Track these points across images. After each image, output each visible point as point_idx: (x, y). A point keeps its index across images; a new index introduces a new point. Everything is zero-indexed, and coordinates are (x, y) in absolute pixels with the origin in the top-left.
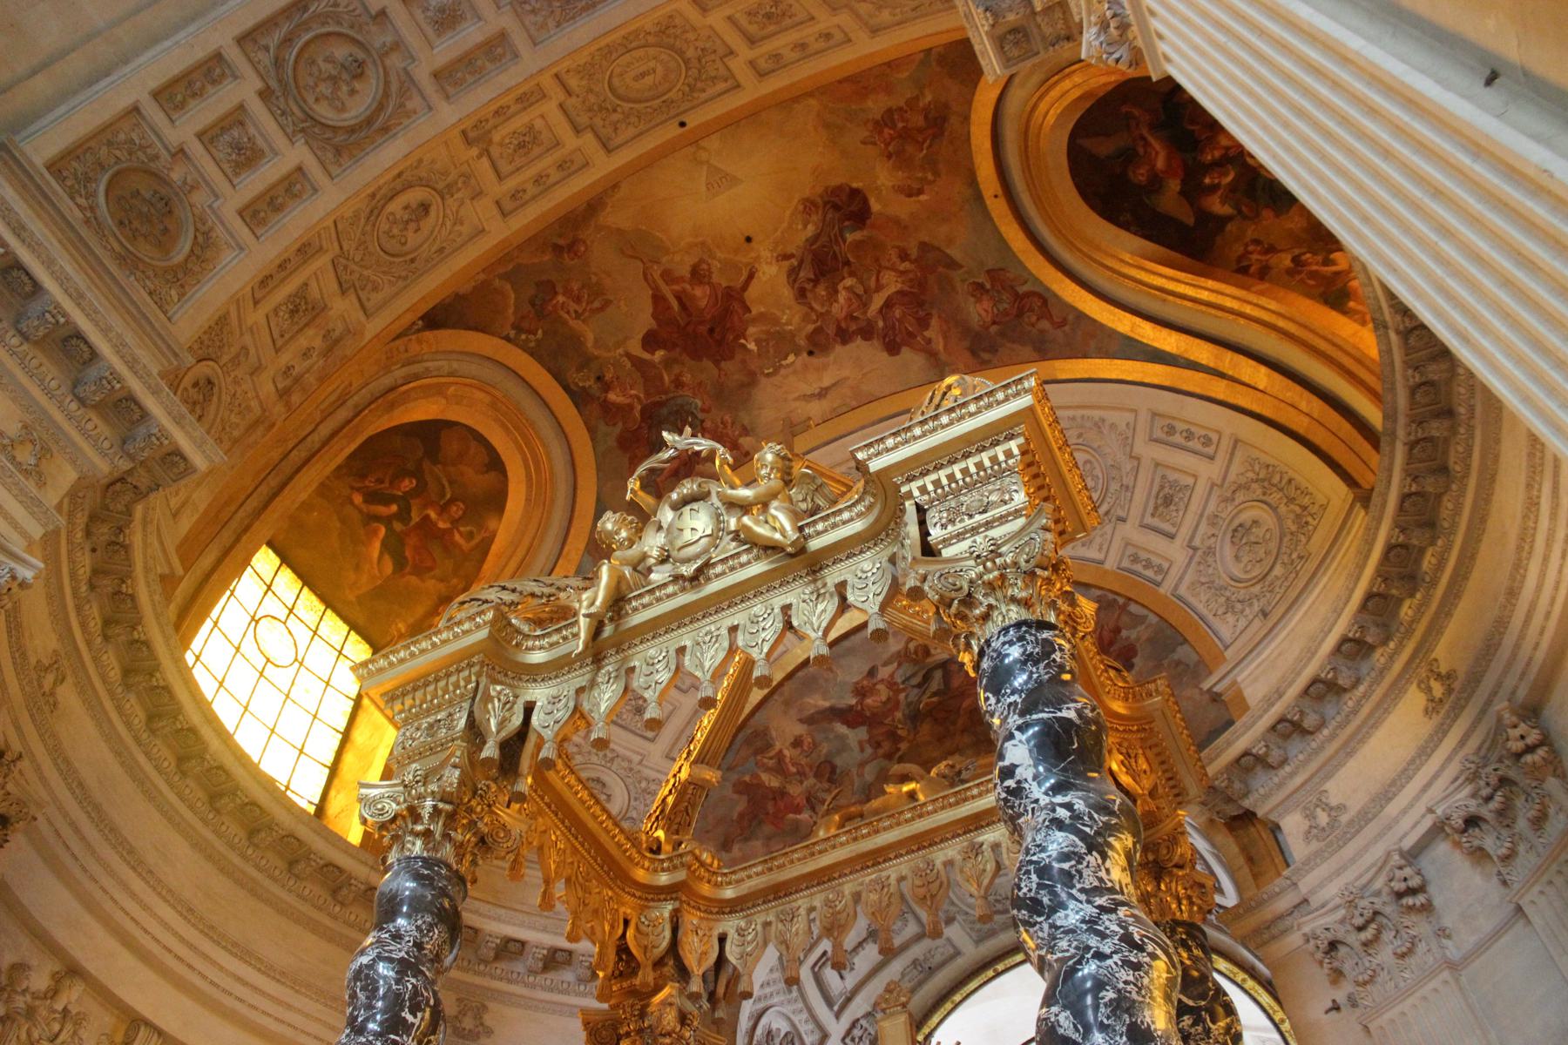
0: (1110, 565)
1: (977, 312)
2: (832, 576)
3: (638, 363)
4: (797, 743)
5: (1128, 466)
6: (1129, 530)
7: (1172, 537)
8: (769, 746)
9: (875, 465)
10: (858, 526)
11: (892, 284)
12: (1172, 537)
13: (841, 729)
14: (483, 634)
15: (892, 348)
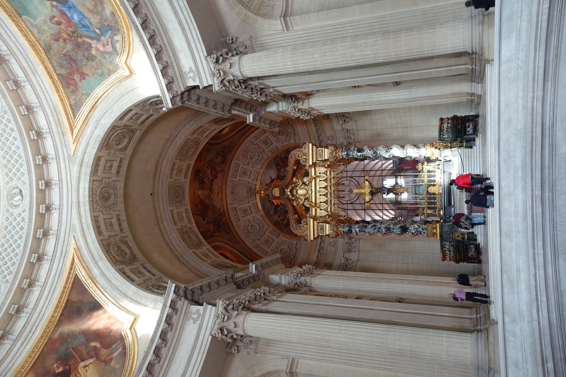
0: (270, 155)
1: (219, 160)
2: (318, 174)
3: (207, 223)
4: (279, 217)
5: (256, 146)
6: (266, 150)
7: (272, 144)
8: (278, 221)
9: (311, 163)
10: (313, 169)
11: (209, 172)
12: (272, 144)
13: (279, 208)
14: (312, 220)
15: (216, 177)
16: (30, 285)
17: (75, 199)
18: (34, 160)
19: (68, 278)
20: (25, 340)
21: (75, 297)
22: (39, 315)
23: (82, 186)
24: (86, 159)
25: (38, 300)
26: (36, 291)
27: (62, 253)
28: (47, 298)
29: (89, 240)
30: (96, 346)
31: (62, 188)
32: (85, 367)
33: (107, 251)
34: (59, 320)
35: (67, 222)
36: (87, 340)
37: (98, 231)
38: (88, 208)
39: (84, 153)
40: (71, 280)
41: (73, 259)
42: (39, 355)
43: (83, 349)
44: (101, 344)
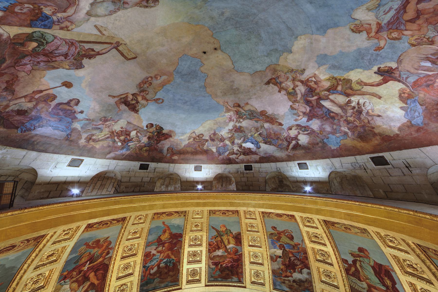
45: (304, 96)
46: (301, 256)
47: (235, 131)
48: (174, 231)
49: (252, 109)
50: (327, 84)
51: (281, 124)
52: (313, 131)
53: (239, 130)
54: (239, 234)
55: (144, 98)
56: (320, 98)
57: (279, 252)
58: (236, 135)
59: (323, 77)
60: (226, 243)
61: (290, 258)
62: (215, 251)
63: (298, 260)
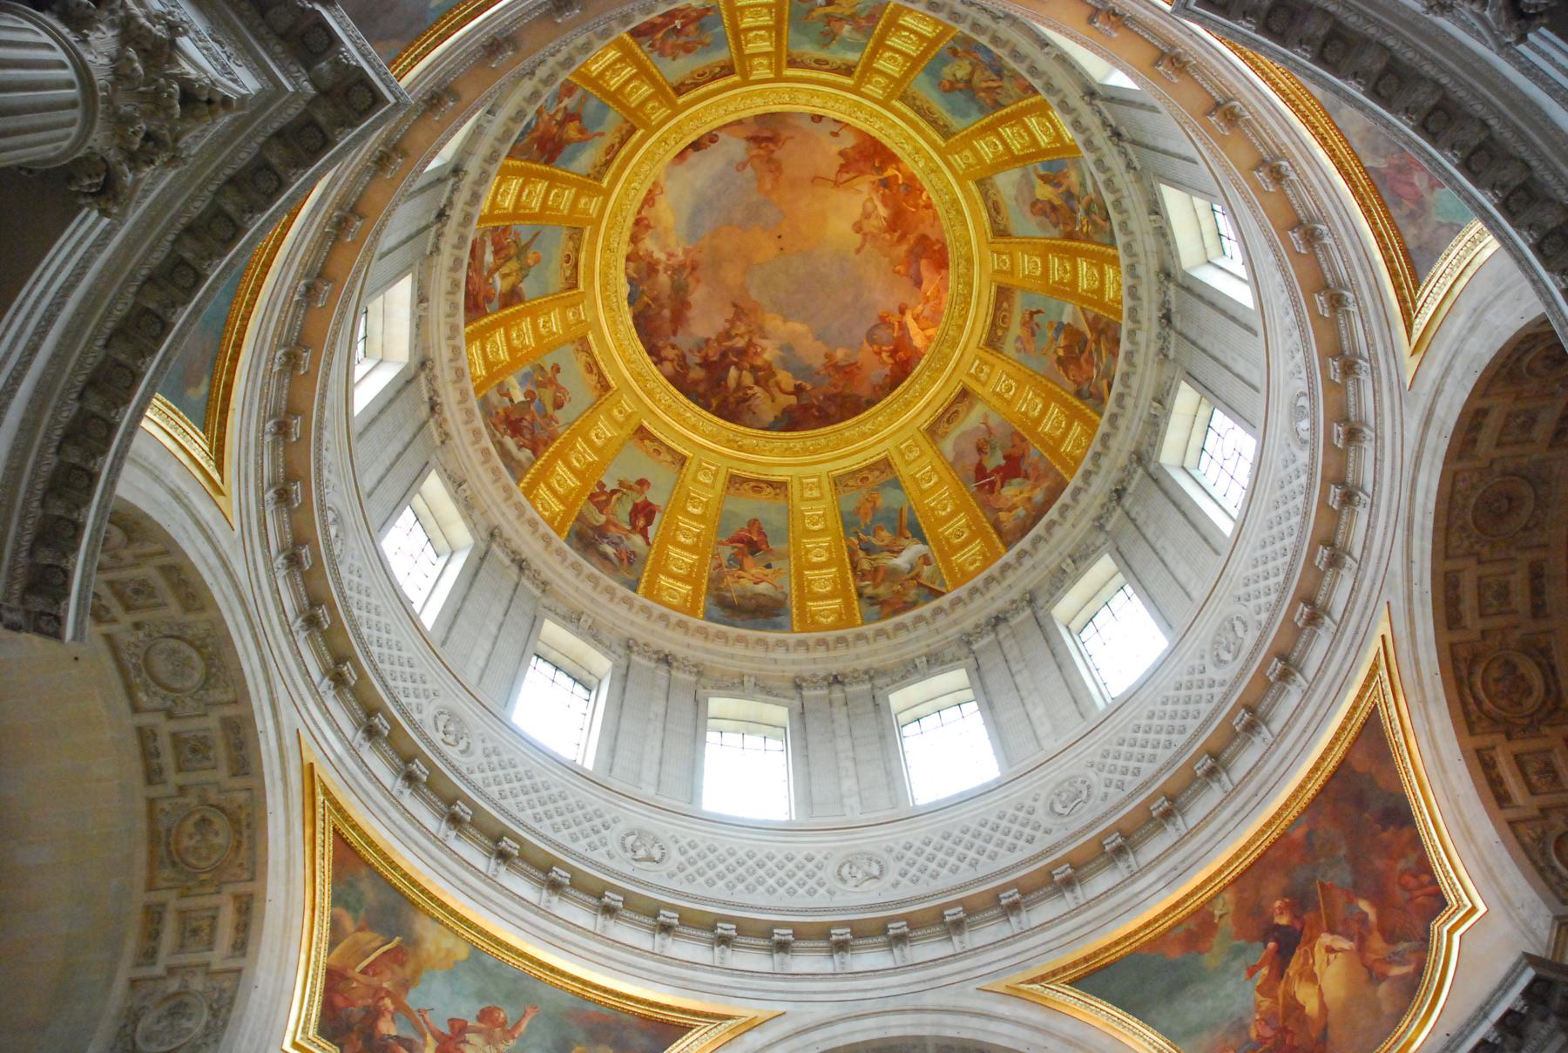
16: (1285, 676)
17: (1404, 502)
18: (1324, 368)
19: (1354, 708)
20: (1242, 808)
21: (1361, 763)
22: (1281, 763)
23: (1422, 479)
24: (1440, 411)
25: (1288, 725)
26: (1293, 697)
27: (1356, 633)
28: (1304, 731)
29: (1419, 633)
30: (1366, 915)
31: (1382, 461)
32: (1330, 950)
33: (1459, 681)
34: (1313, 800)
35: (1380, 557)
36: (1355, 885)
37: (1448, 612)
38: (1428, 546)
39: (1438, 392)
40: (1361, 716)
41: (1375, 667)
42: (1257, 861)
43: (1341, 900)
44: (1380, 917)
45: (732, 349)
46: (543, 435)
47: (649, 263)
48: (568, 149)
49: (691, 287)
50: (759, 362)
51: (675, 333)
52: (685, 376)
53: (652, 268)
54: (521, 300)
55: (758, 156)
56: (736, 364)
57: (519, 396)
58: (643, 265)
59: (767, 356)
60: (505, 270)
61: (521, 419)
62: (494, 243)
63: (533, 433)
